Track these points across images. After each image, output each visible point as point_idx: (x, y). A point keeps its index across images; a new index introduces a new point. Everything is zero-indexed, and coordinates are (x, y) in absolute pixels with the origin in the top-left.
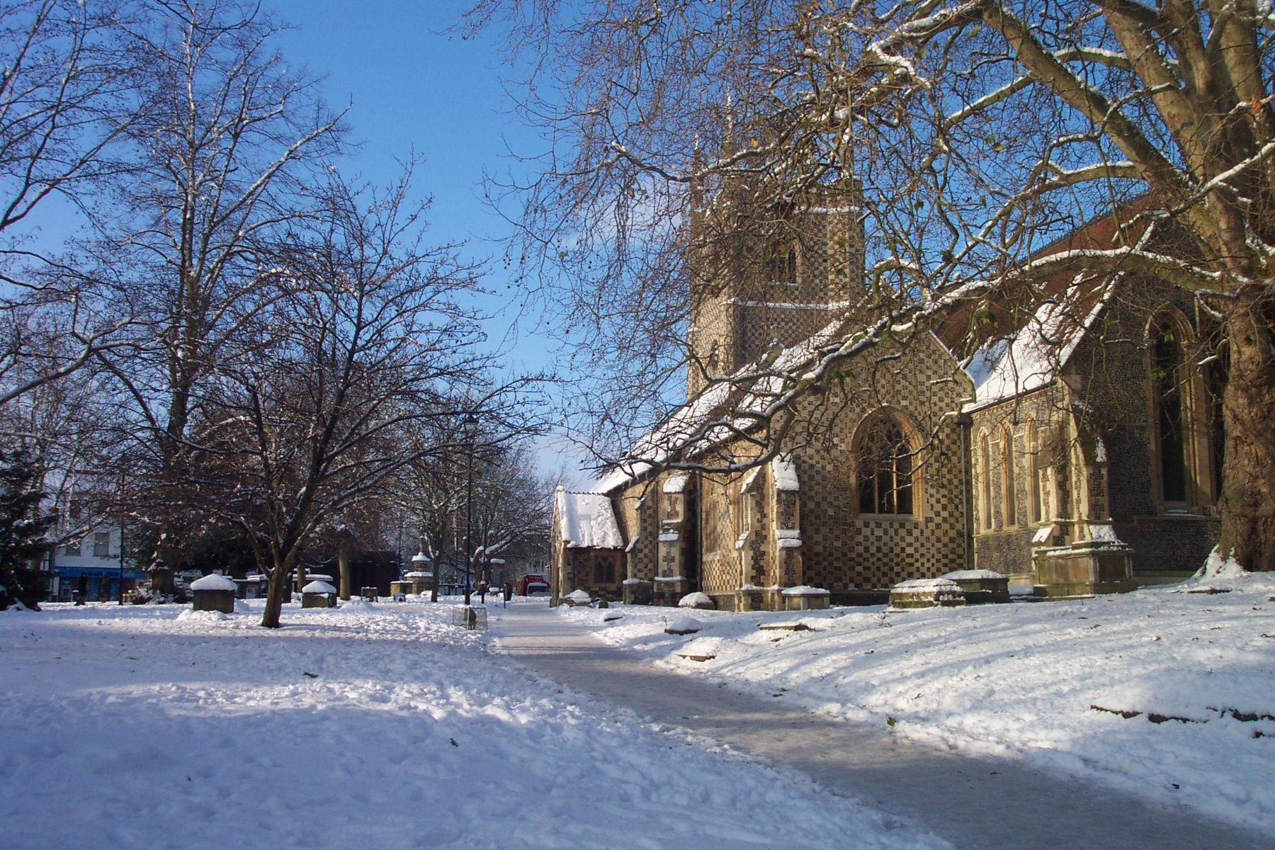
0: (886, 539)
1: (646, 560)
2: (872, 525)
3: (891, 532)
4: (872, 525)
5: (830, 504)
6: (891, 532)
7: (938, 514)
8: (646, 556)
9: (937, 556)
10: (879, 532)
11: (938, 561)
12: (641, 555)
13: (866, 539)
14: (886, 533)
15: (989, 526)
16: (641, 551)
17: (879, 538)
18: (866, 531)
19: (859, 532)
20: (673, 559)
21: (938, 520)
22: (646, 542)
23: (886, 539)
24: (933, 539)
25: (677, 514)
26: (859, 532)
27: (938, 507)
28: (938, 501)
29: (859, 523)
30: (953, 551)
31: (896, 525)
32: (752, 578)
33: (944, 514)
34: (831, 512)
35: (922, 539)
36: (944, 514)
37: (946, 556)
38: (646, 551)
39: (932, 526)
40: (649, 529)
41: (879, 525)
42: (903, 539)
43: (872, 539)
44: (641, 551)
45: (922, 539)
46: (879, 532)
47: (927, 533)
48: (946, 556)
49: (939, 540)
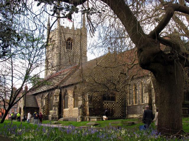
0: (109, 106)
1: (46, 110)
2: (106, 103)
3: (110, 105)
4: (106, 103)
5: (98, 99)
6: (110, 105)
7: (119, 101)
8: (46, 109)
9: (119, 110)
10: (108, 105)
11: (119, 111)
12: (45, 109)
13: (105, 106)
14: (109, 105)
15: (130, 104)
16: (45, 108)
17: (108, 106)
18: (105, 105)
19: (104, 104)
20: (56, 110)
21: (119, 102)
22: (46, 106)
23: (109, 106)
24: (118, 107)
25: (57, 100)
26: (47, 102)
27: (119, 100)
28: (119, 98)
29: (104, 103)
30: (122, 109)
31: (111, 103)
32: (82, 114)
33: (120, 101)
34: (98, 100)
35: (116, 107)
36: (120, 101)
37: (120, 110)
38: (46, 108)
39: (118, 104)
40: (47, 103)
41: (108, 103)
42: (112, 106)
43: (106, 106)
44: (45, 108)
45: (116, 107)
46: (108, 105)
47: (117, 105)
48: (120, 110)
49: (119, 107)
